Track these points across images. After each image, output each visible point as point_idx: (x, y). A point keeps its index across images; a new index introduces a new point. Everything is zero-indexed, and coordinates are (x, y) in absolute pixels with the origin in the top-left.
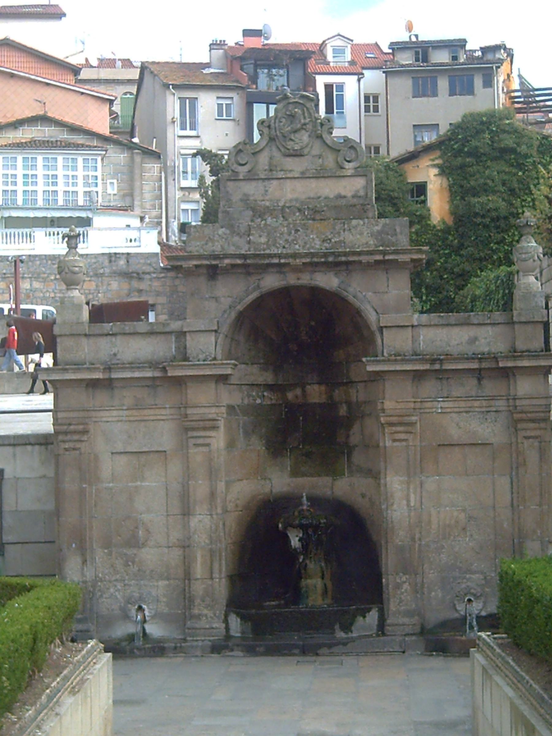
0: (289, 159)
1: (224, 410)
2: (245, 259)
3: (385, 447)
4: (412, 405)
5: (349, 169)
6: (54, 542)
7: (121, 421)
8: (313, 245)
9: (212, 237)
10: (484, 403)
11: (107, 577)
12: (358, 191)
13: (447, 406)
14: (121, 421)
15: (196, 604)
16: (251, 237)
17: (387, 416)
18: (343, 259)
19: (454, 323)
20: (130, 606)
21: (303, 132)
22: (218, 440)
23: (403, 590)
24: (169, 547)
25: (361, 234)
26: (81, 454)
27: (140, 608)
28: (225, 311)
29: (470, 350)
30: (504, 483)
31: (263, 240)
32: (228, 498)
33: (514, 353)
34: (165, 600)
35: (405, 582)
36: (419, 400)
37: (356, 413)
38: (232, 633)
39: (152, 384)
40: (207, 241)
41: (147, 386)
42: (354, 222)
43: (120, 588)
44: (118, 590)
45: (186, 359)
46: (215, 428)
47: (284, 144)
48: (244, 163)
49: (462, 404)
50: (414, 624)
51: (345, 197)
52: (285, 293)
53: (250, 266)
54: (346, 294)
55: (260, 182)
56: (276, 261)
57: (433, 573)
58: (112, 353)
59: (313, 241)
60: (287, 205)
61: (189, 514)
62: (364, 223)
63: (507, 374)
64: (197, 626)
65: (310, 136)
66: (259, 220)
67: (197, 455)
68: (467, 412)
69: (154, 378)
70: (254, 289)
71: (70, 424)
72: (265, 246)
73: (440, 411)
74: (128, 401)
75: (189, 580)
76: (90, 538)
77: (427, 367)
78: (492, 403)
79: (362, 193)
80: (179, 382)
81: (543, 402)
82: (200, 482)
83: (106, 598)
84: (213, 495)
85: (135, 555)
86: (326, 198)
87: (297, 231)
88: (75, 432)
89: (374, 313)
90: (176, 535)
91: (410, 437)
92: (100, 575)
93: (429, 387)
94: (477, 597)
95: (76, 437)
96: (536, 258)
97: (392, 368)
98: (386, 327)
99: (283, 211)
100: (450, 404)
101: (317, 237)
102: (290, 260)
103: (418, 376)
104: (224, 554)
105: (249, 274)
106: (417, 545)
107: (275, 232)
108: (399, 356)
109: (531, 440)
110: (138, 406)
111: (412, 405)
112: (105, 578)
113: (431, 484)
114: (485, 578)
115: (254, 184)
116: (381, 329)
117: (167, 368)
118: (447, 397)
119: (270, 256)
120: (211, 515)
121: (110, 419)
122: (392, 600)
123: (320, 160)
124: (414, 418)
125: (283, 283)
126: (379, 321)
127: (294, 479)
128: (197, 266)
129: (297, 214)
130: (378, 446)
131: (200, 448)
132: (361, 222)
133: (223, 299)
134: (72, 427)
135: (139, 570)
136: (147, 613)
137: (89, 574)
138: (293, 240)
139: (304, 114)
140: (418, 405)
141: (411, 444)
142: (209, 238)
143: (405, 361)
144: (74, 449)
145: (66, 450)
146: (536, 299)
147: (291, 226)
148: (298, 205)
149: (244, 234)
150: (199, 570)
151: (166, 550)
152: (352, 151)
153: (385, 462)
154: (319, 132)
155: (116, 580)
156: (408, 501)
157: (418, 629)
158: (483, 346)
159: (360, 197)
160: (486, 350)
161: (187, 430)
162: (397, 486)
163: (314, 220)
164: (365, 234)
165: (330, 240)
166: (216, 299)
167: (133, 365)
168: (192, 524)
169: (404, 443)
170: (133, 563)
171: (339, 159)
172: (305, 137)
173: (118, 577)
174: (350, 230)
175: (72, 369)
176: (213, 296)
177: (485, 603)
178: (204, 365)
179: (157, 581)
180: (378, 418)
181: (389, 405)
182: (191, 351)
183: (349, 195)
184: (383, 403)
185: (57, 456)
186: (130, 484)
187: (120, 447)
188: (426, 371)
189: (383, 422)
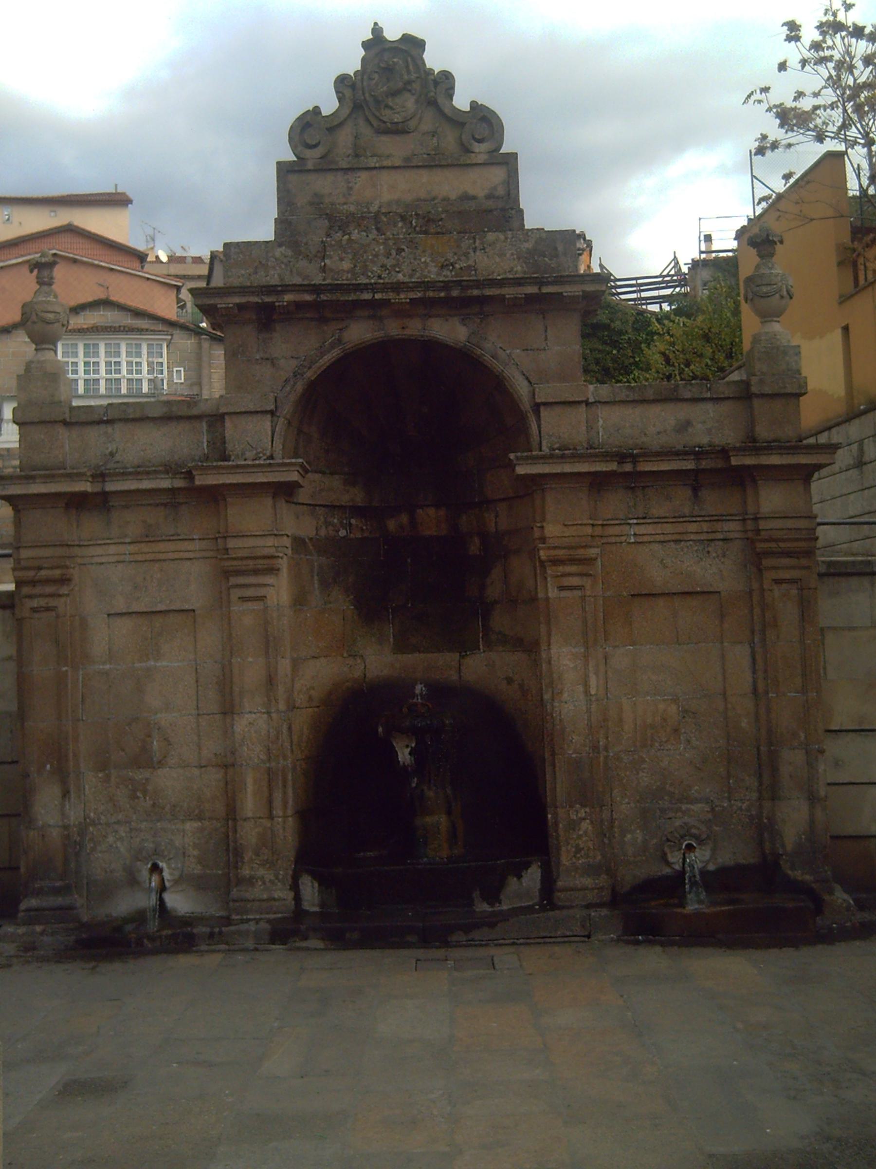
0: (384, 138)
1: (287, 542)
2: (318, 294)
3: (547, 599)
4: (589, 530)
5: (480, 153)
6: (17, 762)
7: (123, 562)
8: (426, 273)
9: (264, 262)
10: (705, 527)
11: (103, 817)
12: (495, 188)
13: (645, 532)
14: (123, 562)
15: (246, 859)
16: (327, 261)
17: (549, 548)
18: (476, 292)
19: (651, 398)
20: (139, 863)
21: (407, 95)
22: (279, 591)
23: (581, 833)
24: (202, 767)
25: (502, 255)
26: (58, 617)
27: (155, 868)
28: (287, 381)
29: (678, 442)
30: (740, 655)
31: (346, 265)
32: (298, 686)
33: (752, 444)
34: (196, 853)
35: (584, 819)
36: (600, 522)
38: (306, 906)
39: (171, 500)
40: (256, 267)
41: (162, 504)
42: (491, 236)
43: (124, 835)
44: (121, 839)
45: (226, 458)
46: (273, 571)
47: (377, 114)
48: (314, 143)
49: (669, 528)
50: (602, 888)
51: (474, 198)
52: (379, 352)
53: (326, 305)
54: (479, 352)
55: (339, 173)
56: (367, 296)
57: (629, 803)
58: (107, 452)
59: (426, 265)
60: (383, 210)
61: (233, 713)
62: (506, 238)
63: (741, 479)
64: (248, 895)
65: (417, 102)
66: (339, 234)
67: (245, 617)
68: (676, 541)
69: (172, 491)
70: (333, 346)
71: (40, 568)
72: (349, 276)
73: (632, 540)
75: (235, 820)
76: (75, 755)
77: (613, 466)
78: (718, 526)
79: (501, 191)
80: (214, 496)
81: (803, 524)
82: (250, 659)
83: (100, 852)
84: (270, 681)
85: (147, 779)
86: (444, 200)
87: (400, 251)
88: (48, 581)
89: (526, 383)
91: (587, 582)
92: (92, 815)
93: (615, 503)
94: (701, 842)
95: (49, 589)
96: (785, 293)
97: (557, 469)
98: (545, 404)
99: (377, 220)
100: (650, 529)
101: (432, 261)
102: (391, 295)
103: (598, 483)
104: (290, 777)
105: (323, 320)
106: (602, 759)
107: (365, 252)
108: (566, 453)
109: (784, 585)
110: (148, 537)
111: (589, 530)
112: (99, 819)
114: (713, 809)
115: (330, 177)
116: (537, 408)
117: (194, 473)
118: (645, 518)
119: (359, 288)
120: (268, 713)
121: (103, 560)
122: (563, 849)
123: (435, 140)
124: (593, 552)
125: (379, 334)
126: (534, 395)
127: (400, 656)
128: (241, 307)
129: (400, 224)
130: (534, 599)
131: (250, 603)
132: (502, 237)
133: (282, 362)
134: (43, 573)
135: (154, 805)
136: (166, 874)
137: (74, 815)
138: (394, 266)
139: (407, 67)
140: (598, 531)
141: (588, 593)
142: (260, 262)
143: (577, 457)
144: (48, 609)
145: (34, 610)
146: (787, 358)
147: (391, 243)
148: (400, 211)
149: (316, 256)
150: (250, 803)
151: (196, 772)
152: (484, 125)
153: (548, 623)
154: (432, 94)
155: (118, 822)
156: (586, 685)
157: (606, 896)
158: (700, 436)
159: (498, 197)
160: (705, 440)
161: (227, 574)
162: (568, 663)
163: (426, 233)
164: (508, 255)
165: (452, 265)
166: (273, 361)
167: (140, 472)
168: (238, 729)
169: (578, 593)
170: (145, 792)
171: (463, 137)
172: (409, 103)
173: (120, 817)
174: (484, 249)
175: (41, 476)
176: (266, 356)
177: (714, 851)
178: (254, 466)
179: (183, 821)
180: (533, 553)
181: (552, 530)
182: (234, 445)
183: (481, 193)
184: (542, 527)
185: (20, 622)
186: (137, 665)
187: (120, 605)
188: (612, 474)
189: (543, 558)
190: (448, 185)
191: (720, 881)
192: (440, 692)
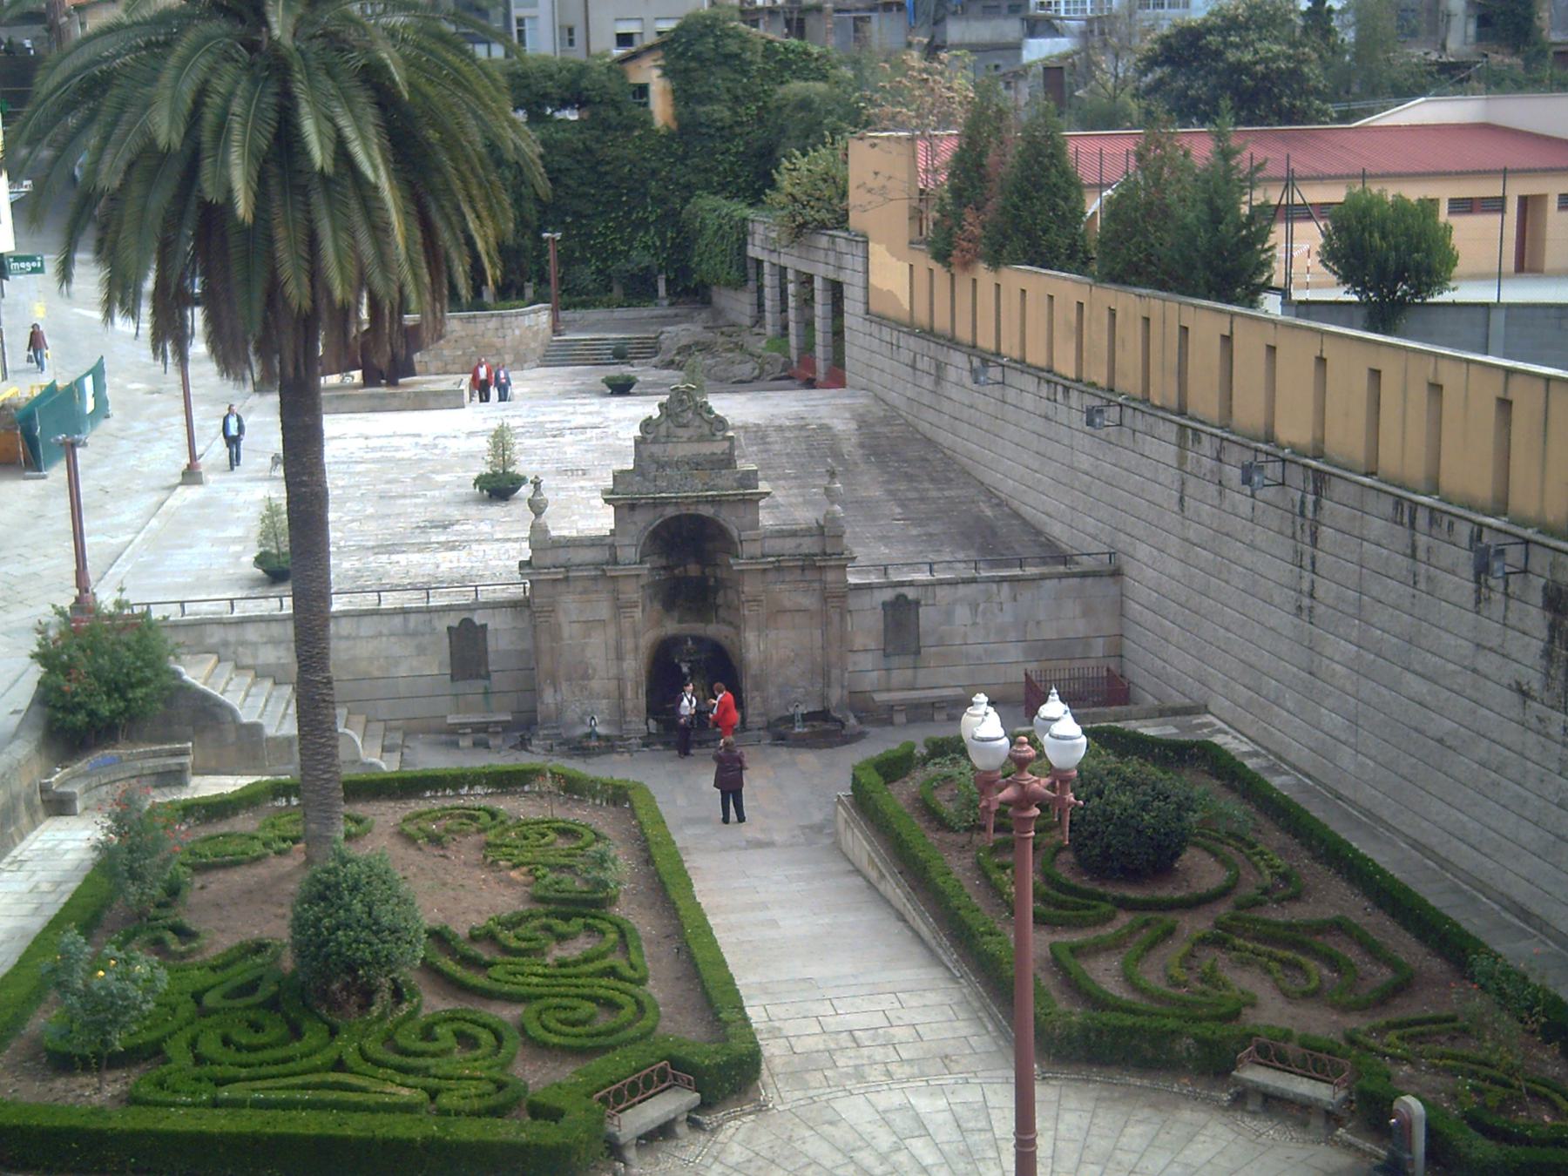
22: (638, 614)
30: (817, 633)
37: (720, 584)
45: (616, 562)
52: (678, 518)
53: (658, 504)
74: (580, 589)
84: (637, 648)
90: (613, 672)
99: (677, 465)
110: (585, 592)
113: (772, 635)
130: (738, 609)
137: (559, 698)
150: (629, 694)
161: (619, 608)
181: (746, 589)
187: (574, 618)
190: (706, 449)
191: (808, 717)
192: (698, 640)
